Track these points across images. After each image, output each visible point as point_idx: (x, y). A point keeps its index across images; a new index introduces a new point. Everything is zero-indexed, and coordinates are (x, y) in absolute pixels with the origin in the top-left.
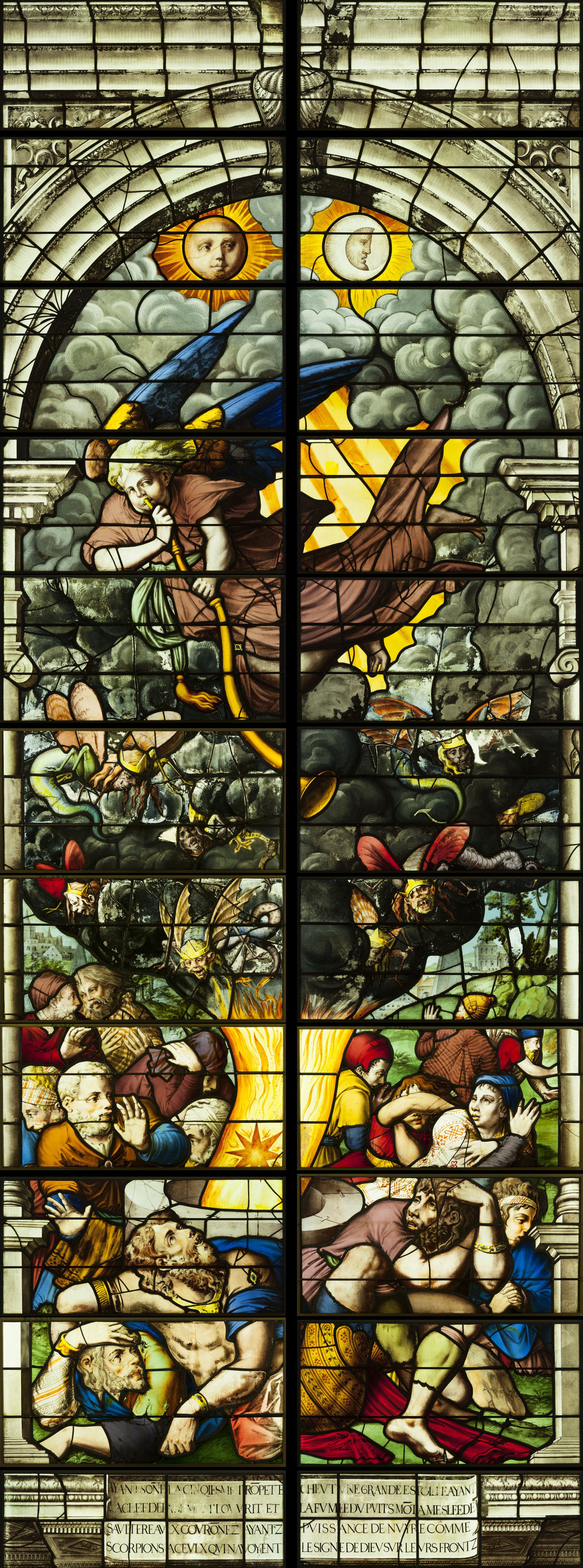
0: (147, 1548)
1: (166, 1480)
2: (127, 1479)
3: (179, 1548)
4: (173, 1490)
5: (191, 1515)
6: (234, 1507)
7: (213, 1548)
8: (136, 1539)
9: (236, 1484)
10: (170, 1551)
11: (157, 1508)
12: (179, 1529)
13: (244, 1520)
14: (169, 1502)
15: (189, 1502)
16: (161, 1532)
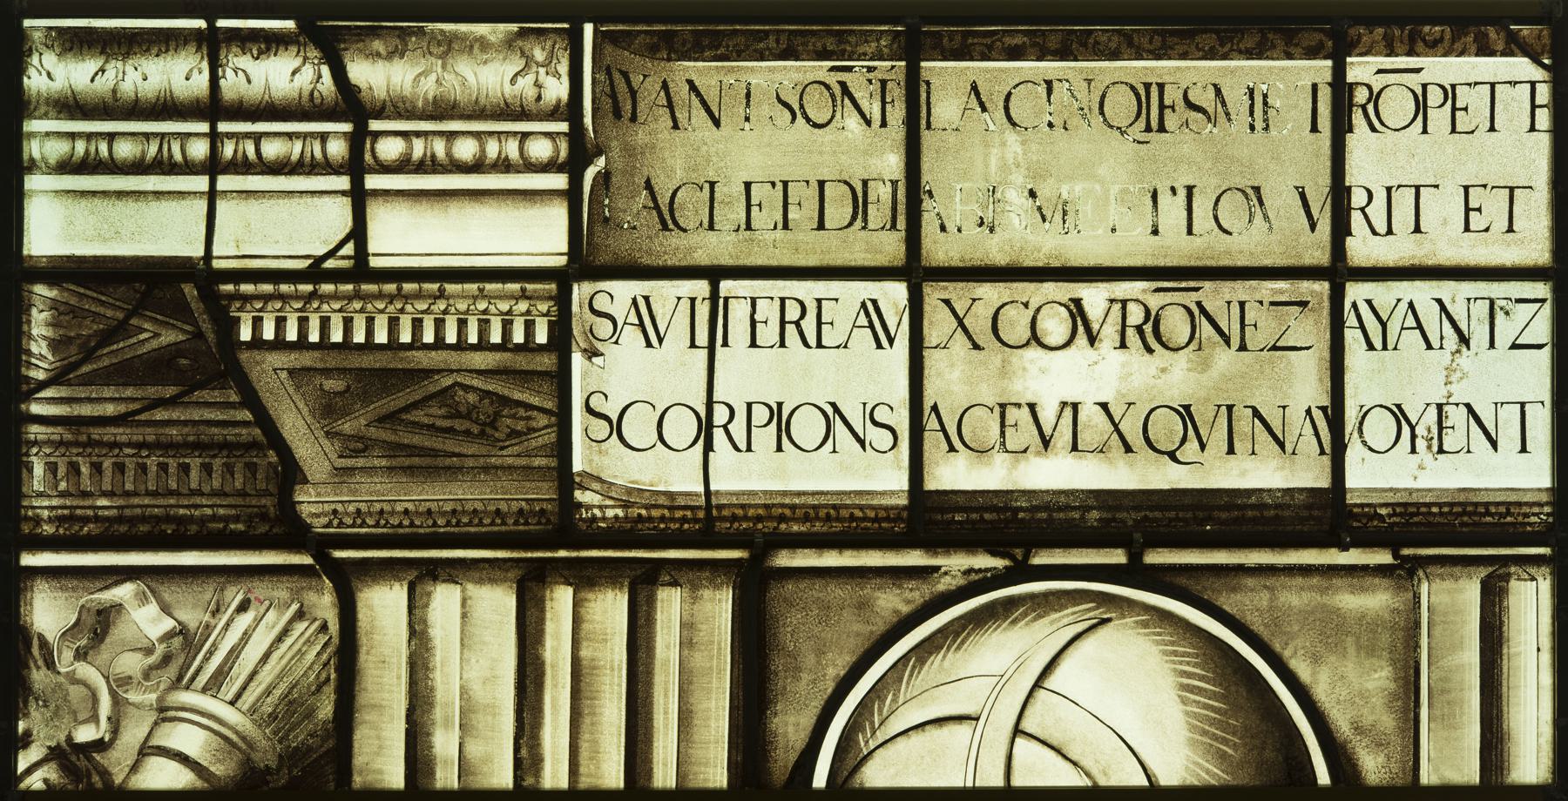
0: (808, 427)
1: (913, 50)
2: (696, 49)
3: (984, 426)
4: (946, 107)
5: (1047, 246)
6: (1282, 201)
7: (1167, 428)
8: (747, 375)
9: (1295, 78)
10: (933, 442)
11: (860, 205)
12: (979, 322)
13: (1339, 272)
14: (927, 177)
15: (1037, 173)
16: (882, 337)
